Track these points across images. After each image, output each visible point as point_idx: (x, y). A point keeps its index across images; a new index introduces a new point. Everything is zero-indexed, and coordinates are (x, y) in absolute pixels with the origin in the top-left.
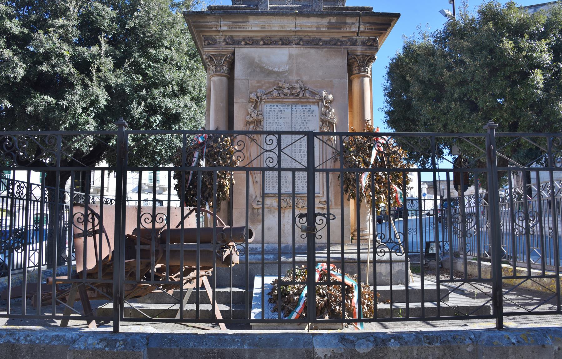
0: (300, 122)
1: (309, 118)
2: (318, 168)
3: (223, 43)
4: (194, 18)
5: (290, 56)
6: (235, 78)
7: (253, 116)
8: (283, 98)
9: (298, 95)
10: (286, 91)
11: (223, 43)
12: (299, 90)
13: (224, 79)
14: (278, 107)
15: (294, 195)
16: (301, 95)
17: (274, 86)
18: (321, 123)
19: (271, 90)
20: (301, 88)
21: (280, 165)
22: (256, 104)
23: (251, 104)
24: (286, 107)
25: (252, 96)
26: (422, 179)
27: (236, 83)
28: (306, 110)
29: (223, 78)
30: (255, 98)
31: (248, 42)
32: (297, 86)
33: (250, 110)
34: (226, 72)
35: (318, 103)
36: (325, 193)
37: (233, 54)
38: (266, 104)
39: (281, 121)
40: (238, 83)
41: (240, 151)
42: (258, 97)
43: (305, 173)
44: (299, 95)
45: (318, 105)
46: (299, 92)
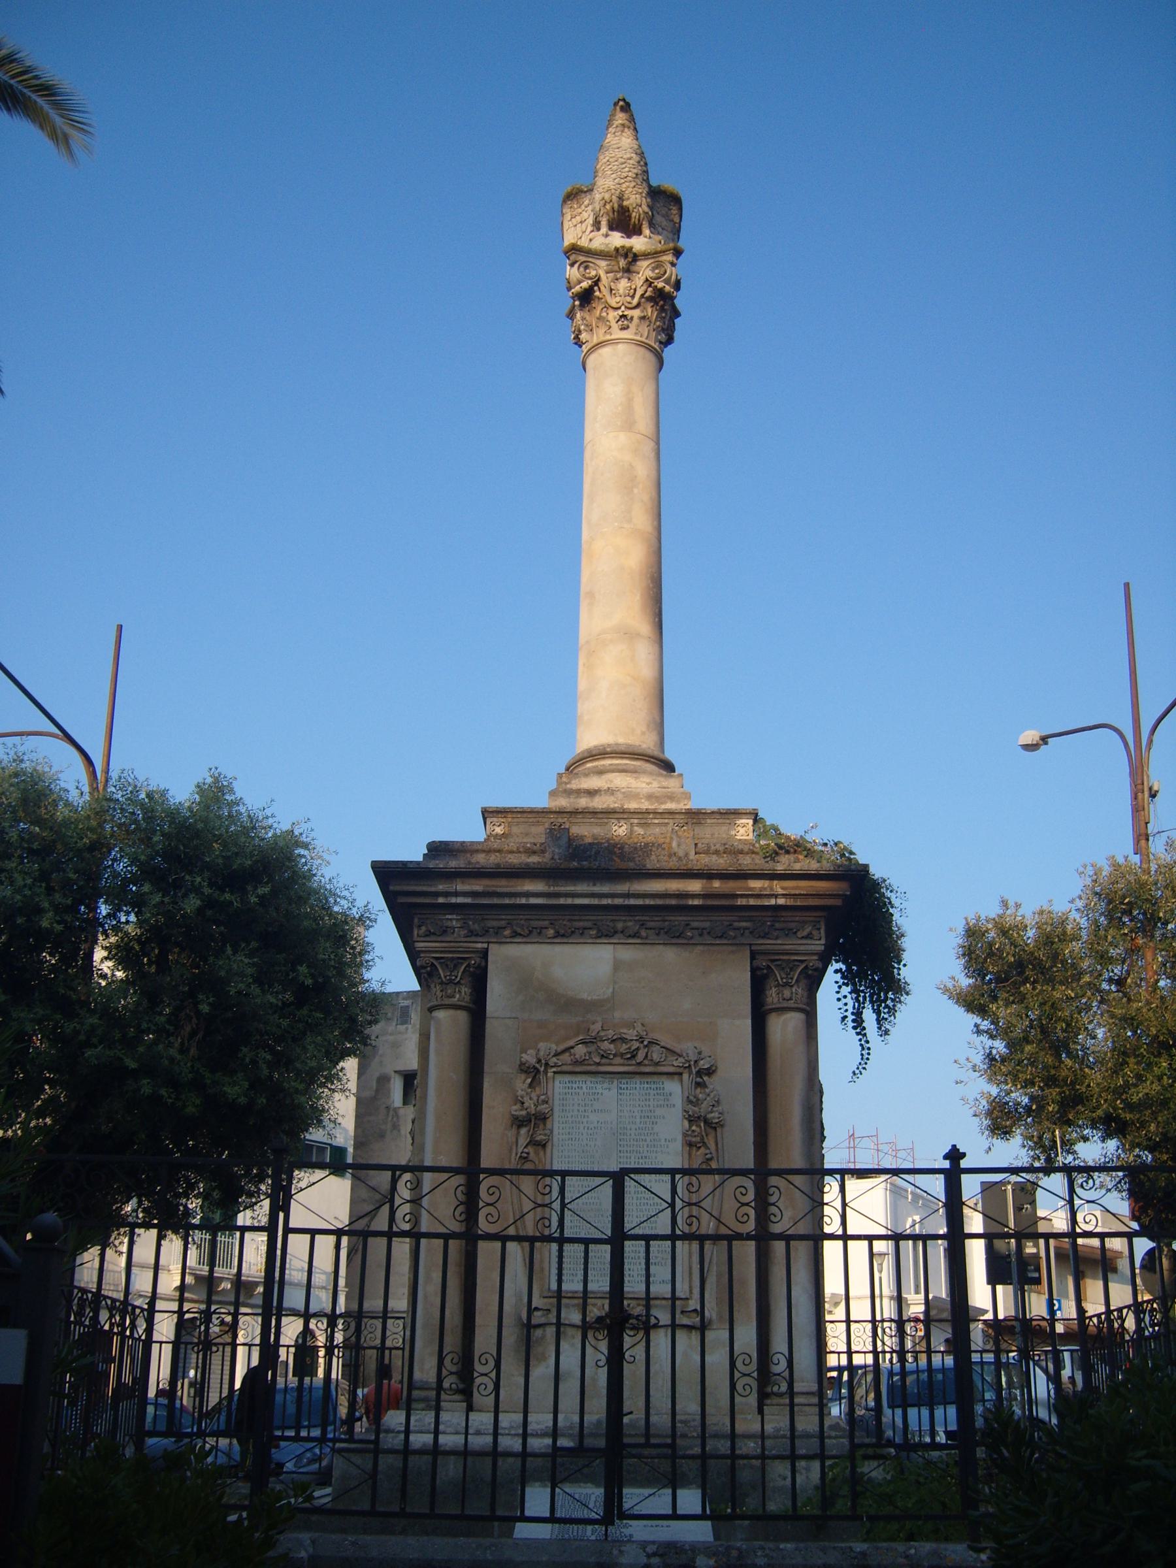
0: (638, 1120)
1: (659, 1112)
2: (632, 1232)
4: (388, 875)
5: (617, 966)
6: (488, 1015)
7: (526, 1105)
8: (598, 1064)
9: (633, 1057)
10: (606, 1045)
12: (636, 1045)
13: (462, 1017)
14: (585, 1085)
15: (385, 1315)
16: (640, 1056)
17: (577, 1035)
18: (686, 1123)
19: (571, 1043)
20: (641, 1039)
21: (845, 1229)
23: (523, 1076)
24: (606, 1085)
25: (525, 1057)
26: (875, 1250)
27: (491, 1027)
28: (652, 1092)
29: (459, 1012)
30: (533, 1061)
31: (519, 930)
32: (631, 1034)
33: (520, 1093)
34: (467, 998)
35: (681, 1074)
36: (696, 1291)
37: (485, 954)
38: (559, 1078)
39: (593, 1118)
41: (743, 1204)
42: (539, 1061)
43: (608, 1247)
45: (681, 1081)
46: (638, 1049)
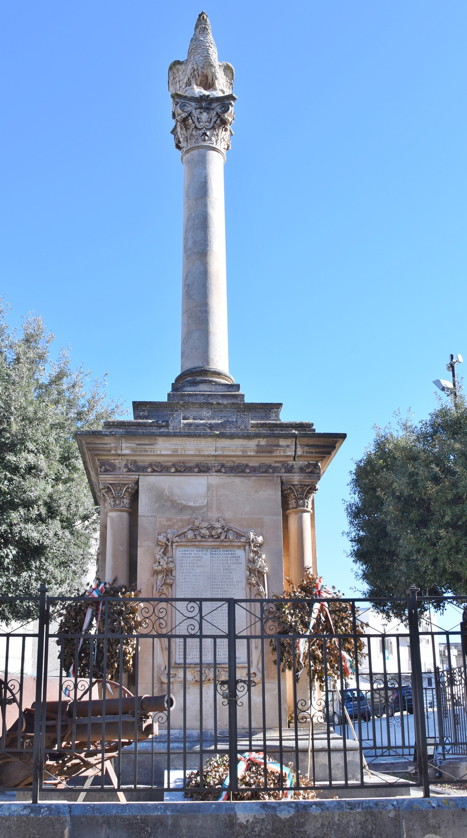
0: (222, 571)
1: (233, 566)
3: (125, 470)
5: (209, 487)
6: (140, 514)
7: (161, 563)
8: (201, 541)
9: (219, 537)
10: (204, 531)
11: (125, 470)
12: (220, 531)
13: (125, 515)
14: (193, 552)
16: (222, 537)
17: (188, 524)
18: (248, 573)
19: (185, 530)
20: (223, 528)
22: (166, 548)
23: (159, 548)
24: (204, 552)
25: (161, 538)
28: (229, 556)
30: (164, 540)
31: (156, 469)
32: (218, 525)
33: (158, 557)
34: (127, 506)
35: (245, 546)
37: (137, 483)
40: (142, 521)
42: (168, 540)
44: (221, 536)
45: (245, 550)
46: (221, 533)
